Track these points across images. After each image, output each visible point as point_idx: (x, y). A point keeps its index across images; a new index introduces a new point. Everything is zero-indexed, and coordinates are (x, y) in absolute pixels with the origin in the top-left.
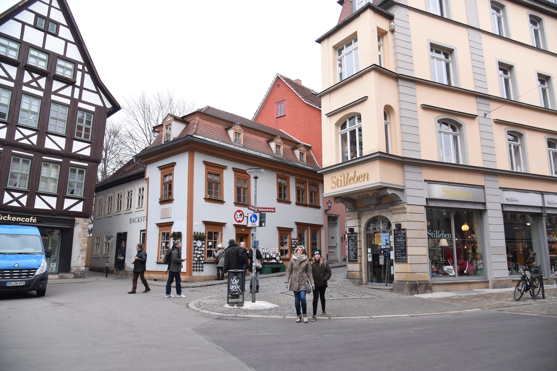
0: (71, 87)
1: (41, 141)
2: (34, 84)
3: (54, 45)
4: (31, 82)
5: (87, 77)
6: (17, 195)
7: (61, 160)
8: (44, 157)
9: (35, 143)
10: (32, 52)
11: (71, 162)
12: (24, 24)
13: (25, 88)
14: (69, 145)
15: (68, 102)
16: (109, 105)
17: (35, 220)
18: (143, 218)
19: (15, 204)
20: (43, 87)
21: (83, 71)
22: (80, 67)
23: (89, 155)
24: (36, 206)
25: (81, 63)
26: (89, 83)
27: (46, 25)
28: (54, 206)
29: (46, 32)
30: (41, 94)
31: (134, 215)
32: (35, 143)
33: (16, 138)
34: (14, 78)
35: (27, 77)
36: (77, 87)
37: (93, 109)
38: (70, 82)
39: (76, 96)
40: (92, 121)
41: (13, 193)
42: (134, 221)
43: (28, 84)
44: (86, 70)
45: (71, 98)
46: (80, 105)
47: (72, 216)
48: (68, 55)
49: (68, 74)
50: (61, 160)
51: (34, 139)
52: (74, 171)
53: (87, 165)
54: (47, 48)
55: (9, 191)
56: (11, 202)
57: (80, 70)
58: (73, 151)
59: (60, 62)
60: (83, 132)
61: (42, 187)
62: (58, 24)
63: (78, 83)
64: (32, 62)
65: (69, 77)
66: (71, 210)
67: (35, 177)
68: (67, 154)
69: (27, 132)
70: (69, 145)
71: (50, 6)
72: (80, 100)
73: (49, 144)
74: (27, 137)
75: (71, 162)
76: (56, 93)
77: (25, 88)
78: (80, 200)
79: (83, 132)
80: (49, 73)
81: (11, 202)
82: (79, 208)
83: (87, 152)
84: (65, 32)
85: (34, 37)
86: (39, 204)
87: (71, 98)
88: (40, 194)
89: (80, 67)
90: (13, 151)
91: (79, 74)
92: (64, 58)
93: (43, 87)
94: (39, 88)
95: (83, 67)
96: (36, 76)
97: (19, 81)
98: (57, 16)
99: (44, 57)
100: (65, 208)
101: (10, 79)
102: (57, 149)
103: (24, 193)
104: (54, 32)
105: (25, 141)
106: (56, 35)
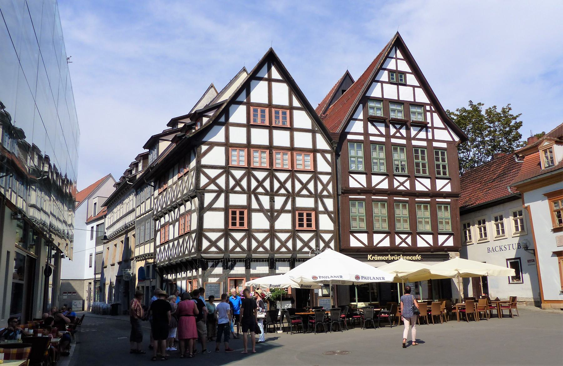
0: (425, 129)
1: (413, 185)
2: (398, 135)
3: (406, 94)
4: (396, 133)
5: (435, 115)
6: (404, 236)
7: (429, 200)
8: (416, 199)
9: (409, 188)
10: (392, 107)
11: (437, 200)
12: (382, 82)
13: (393, 140)
14: (433, 184)
15: (424, 144)
16: (457, 139)
17: (419, 258)
18: (507, 247)
19: (404, 245)
20: (405, 136)
21: (431, 111)
22: (428, 108)
23: (450, 191)
24: (419, 246)
25: (427, 104)
26: (438, 122)
27: (398, 79)
28: (431, 243)
29: (398, 84)
30: (404, 142)
31: (492, 244)
32: (409, 188)
33: (395, 186)
34: (384, 134)
35: (393, 130)
36: (430, 128)
37: (444, 145)
38: (423, 126)
39: (430, 137)
40: (446, 156)
41: (401, 235)
42: (494, 250)
43: (394, 136)
44: (433, 110)
45: (427, 140)
46: (435, 144)
47: (446, 251)
48: (418, 100)
49: (420, 118)
50: (429, 200)
51: (407, 185)
52: (440, 208)
53: (449, 200)
54: (401, 98)
55: (398, 233)
56: (401, 243)
57: (428, 111)
58: (438, 189)
59: (413, 109)
60: (421, 168)
61: (420, 228)
62: (404, 73)
63: (429, 125)
64: (393, 115)
65: (421, 120)
66: (445, 245)
67: (413, 220)
68: (433, 194)
69: (402, 179)
70: (433, 184)
71: (397, 59)
72: (434, 140)
73: (419, 188)
74: (402, 184)
75: (437, 200)
76: (415, 138)
77: (393, 140)
78: (450, 234)
79: (421, 168)
80: (407, 121)
81: (401, 243)
82: (450, 243)
83: (448, 189)
84: (411, 79)
85: (390, 92)
86: (421, 243)
87: (427, 140)
88: (419, 234)
89: (428, 108)
90: (395, 198)
91: (428, 114)
92: (415, 104)
93: (405, 136)
94: (402, 137)
95: (431, 108)
96: (398, 126)
97: (388, 136)
98: (404, 66)
99: (400, 108)
100: (440, 243)
101: (381, 135)
102: (425, 189)
103: (409, 233)
104: (403, 82)
105: (401, 188)
106: (405, 85)
